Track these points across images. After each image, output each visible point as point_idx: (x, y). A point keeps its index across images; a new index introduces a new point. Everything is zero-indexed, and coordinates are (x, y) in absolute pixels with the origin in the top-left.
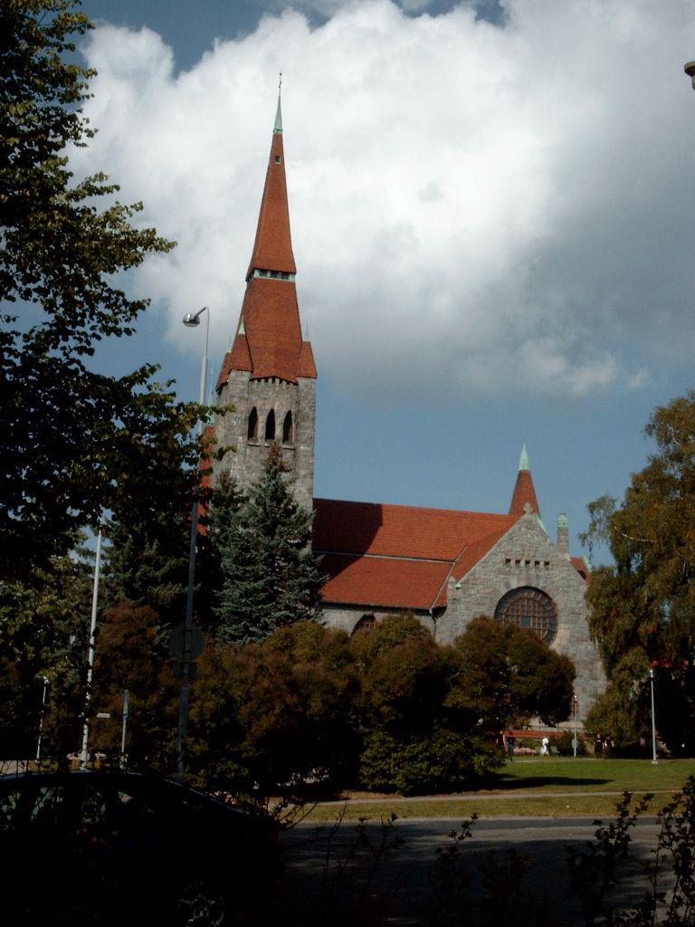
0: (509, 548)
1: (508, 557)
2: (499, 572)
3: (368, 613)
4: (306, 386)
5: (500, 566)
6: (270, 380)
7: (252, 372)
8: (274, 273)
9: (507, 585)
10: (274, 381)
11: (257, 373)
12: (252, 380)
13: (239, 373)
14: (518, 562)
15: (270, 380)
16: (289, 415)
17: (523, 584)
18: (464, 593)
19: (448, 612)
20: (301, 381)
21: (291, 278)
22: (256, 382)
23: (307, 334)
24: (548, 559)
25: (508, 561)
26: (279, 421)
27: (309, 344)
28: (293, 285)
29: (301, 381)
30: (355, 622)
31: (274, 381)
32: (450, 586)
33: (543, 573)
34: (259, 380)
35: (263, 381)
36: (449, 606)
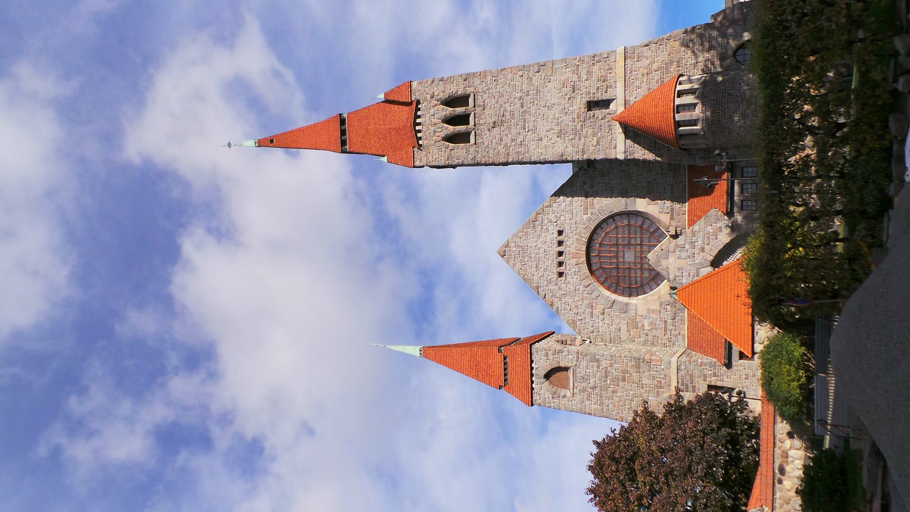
6: (418, 128)
15: (418, 128)
22: (421, 142)
26: (449, 111)
35: (419, 135)
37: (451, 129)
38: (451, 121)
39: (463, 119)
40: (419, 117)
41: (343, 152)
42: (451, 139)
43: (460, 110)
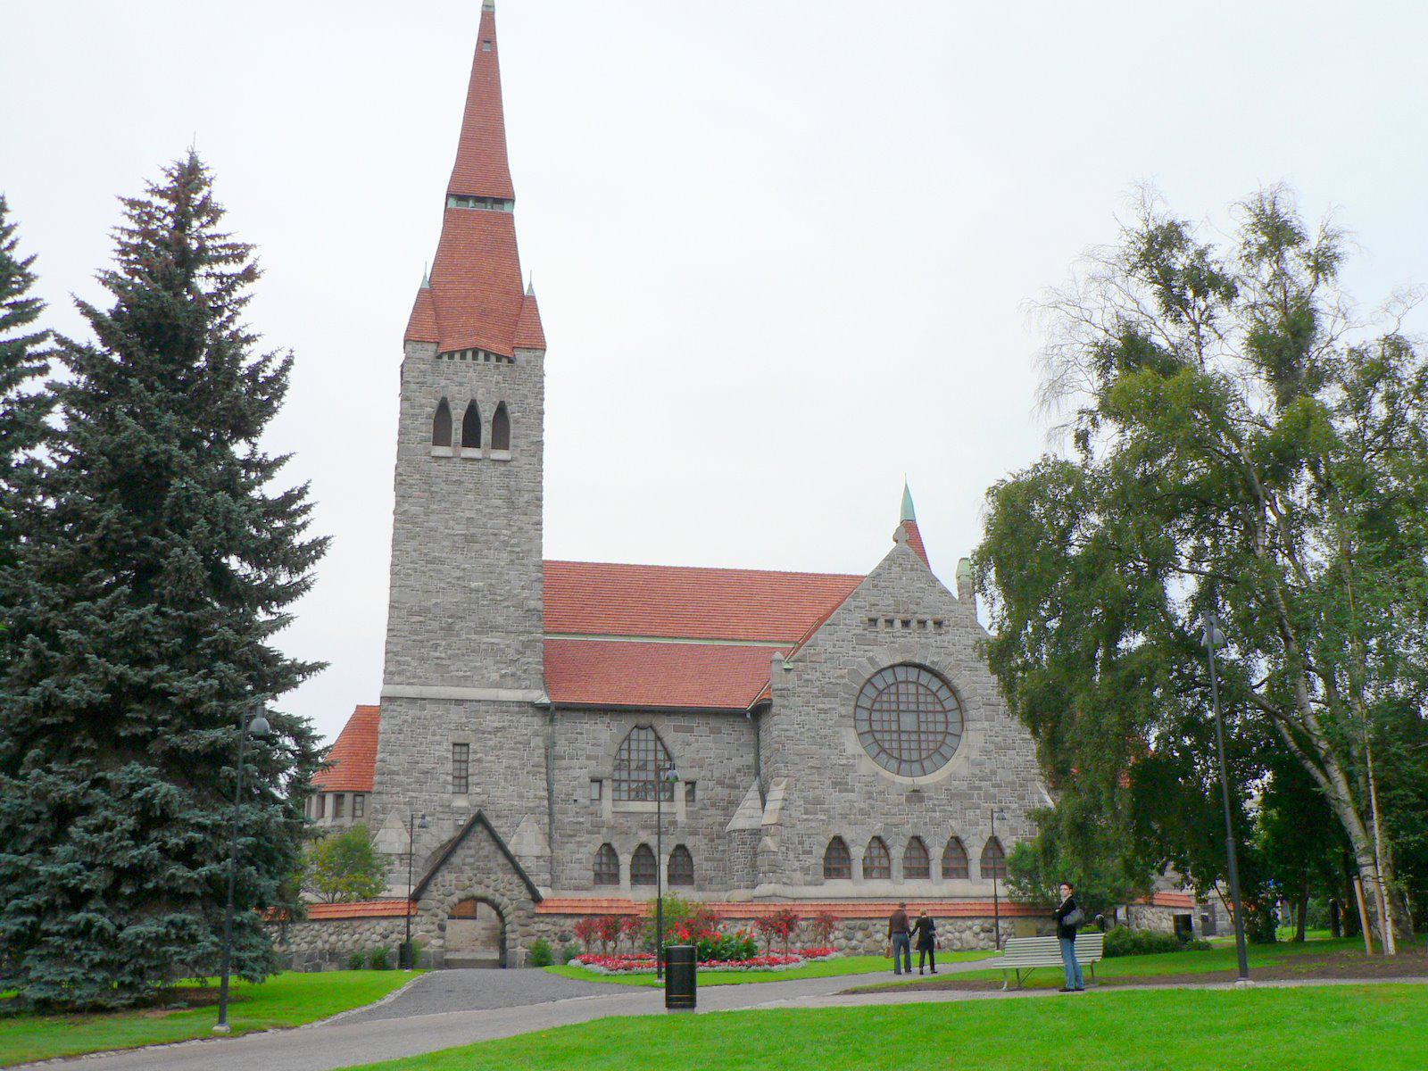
0: (872, 599)
1: (873, 615)
2: (861, 640)
3: (644, 720)
4: (528, 362)
6: (469, 354)
8: (480, 200)
9: (871, 660)
10: (475, 356)
11: (450, 344)
12: (440, 357)
13: (419, 346)
14: (890, 622)
15: (469, 354)
16: (501, 410)
17: (899, 660)
18: (799, 677)
19: (774, 710)
20: (521, 356)
21: (507, 208)
22: (445, 358)
23: (530, 285)
24: (939, 617)
26: (487, 414)
27: (533, 300)
28: (510, 217)
29: (521, 356)
31: (475, 356)
34: (451, 355)
35: (457, 356)
36: (776, 701)
37: (458, 414)
39: (471, 439)
40: (487, 358)
41: (449, 195)
42: (443, 408)
43: (486, 433)
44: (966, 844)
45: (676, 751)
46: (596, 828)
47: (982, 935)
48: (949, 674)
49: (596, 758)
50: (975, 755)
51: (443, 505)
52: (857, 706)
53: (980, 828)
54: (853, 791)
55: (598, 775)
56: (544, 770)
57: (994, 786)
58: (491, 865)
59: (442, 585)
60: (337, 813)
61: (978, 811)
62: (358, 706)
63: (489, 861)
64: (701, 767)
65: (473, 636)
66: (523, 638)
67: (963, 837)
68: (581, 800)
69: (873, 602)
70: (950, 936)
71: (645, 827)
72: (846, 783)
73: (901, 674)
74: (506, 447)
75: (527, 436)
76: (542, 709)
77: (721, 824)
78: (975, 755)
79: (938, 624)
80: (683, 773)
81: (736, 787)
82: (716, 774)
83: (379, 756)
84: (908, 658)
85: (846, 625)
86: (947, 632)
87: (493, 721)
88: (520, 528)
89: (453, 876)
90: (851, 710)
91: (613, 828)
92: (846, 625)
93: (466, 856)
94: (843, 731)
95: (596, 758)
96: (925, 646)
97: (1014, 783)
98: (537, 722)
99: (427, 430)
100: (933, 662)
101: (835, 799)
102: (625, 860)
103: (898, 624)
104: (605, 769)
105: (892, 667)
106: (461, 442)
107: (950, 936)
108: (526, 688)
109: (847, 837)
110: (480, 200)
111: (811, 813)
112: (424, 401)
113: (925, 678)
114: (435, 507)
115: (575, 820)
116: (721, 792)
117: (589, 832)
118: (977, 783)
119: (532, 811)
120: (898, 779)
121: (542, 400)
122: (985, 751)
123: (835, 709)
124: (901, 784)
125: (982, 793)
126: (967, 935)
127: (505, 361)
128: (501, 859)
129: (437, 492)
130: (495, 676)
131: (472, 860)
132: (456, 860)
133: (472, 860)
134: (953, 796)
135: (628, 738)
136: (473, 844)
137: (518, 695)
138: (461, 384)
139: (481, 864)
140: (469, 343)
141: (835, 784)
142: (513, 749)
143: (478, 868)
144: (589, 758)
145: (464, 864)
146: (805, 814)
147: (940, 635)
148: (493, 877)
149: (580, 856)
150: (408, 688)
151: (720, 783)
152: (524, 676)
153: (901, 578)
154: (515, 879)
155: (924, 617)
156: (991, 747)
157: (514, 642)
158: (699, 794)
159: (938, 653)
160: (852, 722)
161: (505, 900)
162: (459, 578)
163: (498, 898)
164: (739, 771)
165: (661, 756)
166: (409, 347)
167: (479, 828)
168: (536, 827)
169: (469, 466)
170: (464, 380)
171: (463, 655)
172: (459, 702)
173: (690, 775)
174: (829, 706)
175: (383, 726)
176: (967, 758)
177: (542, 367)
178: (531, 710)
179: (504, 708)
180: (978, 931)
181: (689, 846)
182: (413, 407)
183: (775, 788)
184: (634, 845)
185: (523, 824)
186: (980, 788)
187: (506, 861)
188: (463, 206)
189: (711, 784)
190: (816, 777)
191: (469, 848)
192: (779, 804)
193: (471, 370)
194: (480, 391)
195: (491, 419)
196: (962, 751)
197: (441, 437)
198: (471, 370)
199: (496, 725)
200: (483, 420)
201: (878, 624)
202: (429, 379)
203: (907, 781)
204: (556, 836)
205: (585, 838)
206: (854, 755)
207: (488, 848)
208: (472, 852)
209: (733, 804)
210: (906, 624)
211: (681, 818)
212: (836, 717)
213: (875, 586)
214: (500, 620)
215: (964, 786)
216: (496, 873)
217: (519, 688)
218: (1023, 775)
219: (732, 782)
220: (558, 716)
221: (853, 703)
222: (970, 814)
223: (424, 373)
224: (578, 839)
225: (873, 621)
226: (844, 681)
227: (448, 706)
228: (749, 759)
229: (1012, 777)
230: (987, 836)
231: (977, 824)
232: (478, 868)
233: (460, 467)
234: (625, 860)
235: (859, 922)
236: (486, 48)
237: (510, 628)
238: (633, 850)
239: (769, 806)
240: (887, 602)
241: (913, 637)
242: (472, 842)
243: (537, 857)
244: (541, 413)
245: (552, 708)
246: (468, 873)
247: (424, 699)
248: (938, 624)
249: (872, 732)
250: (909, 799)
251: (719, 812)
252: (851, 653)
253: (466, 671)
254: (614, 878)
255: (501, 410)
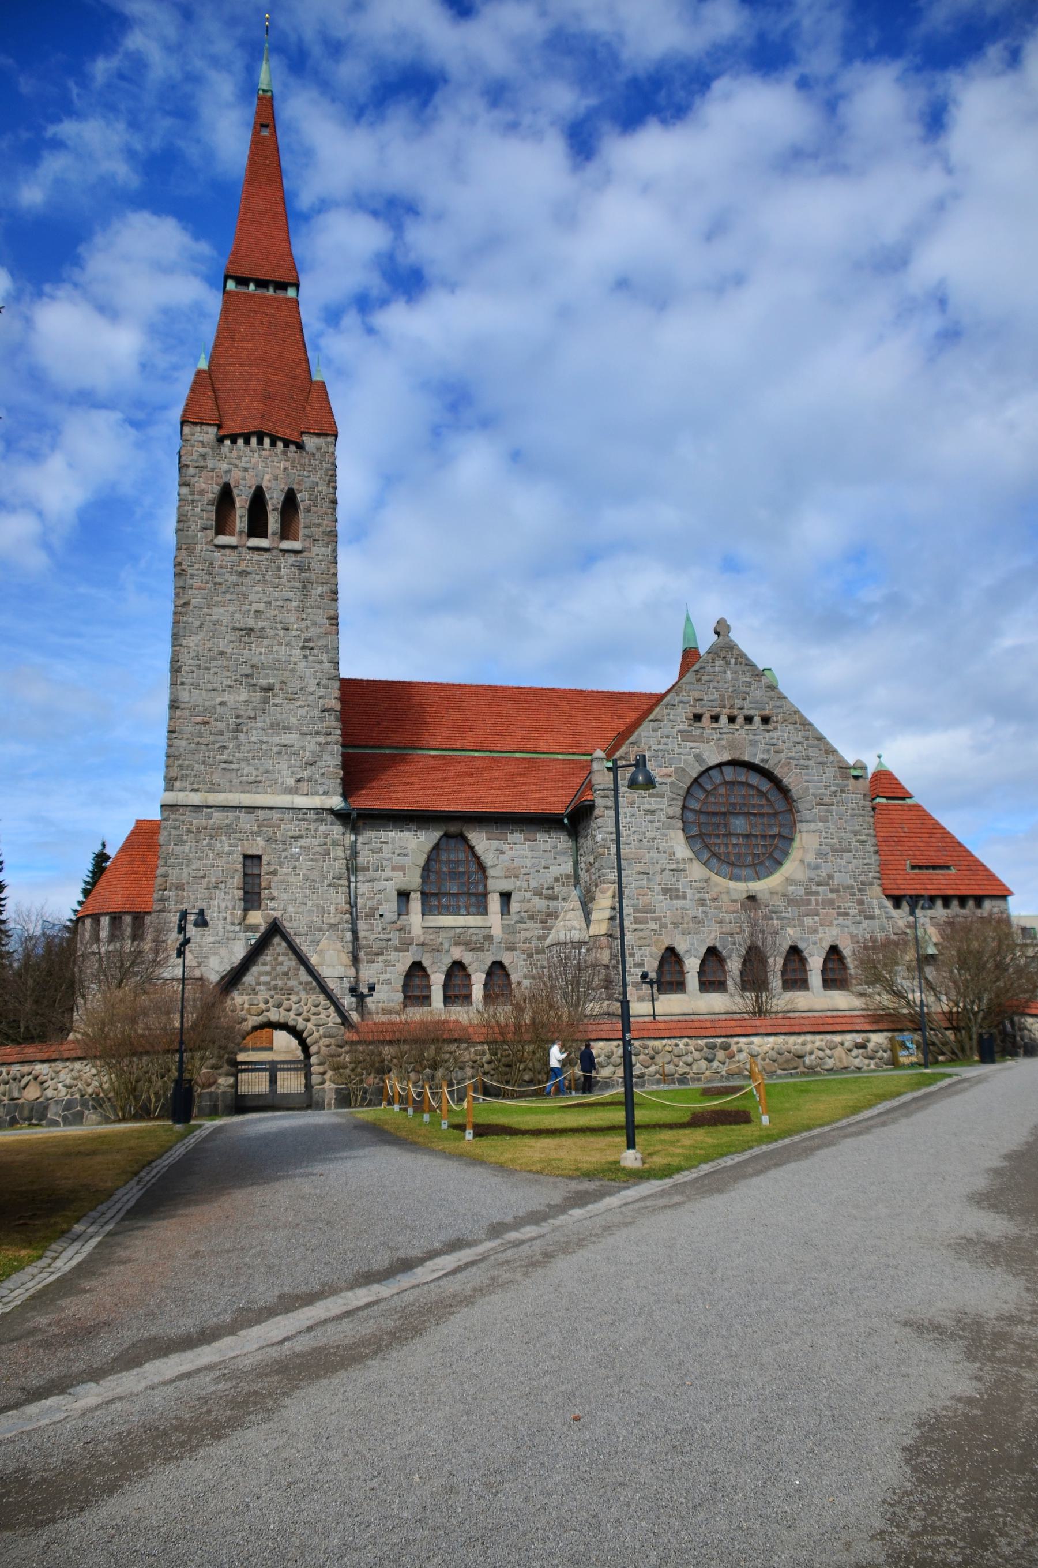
0: (697, 695)
2: (687, 737)
3: (453, 829)
4: (319, 449)
5: (684, 726)
6: (254, 441)
7: (219, 427)
8: (262, 284)
9: (698, 758)
10: (260, 442)
11: (232, 427)
12: (220, 440)
13: (198, 429)
14: (715, 718)
15: (254, 441)
16: (290, 501)
17: (726, 757)
21: (291, 293)
22: (227, 442)
24: (767, 712)
25: (698, 717)
26: (274, 500)
30: (429, 846)
31: (260, 442)
32: (596, 766)
33: (763, 737)
34: (234, 442)
37: (242, 502)
38: (258, 499)
39: (257, 526)
40: (273, 444)
41: (227, 277)
43: (273, 523)
44: (806, 954)
45: (488, 859)
46: (404, 946)
47: (855, 1052)
48: (777, 772)
49: (401, 868)
50: (811, 858)
51: (228, 596)
52: (684, 808)
53: (820, 935)
54: (684, 898)
55: (404, 887)
56: (346, 883)
57: (832, 891)
58: (292, 983)
59: (229, 683)
60: (112, 938)
61: (816, 917)
62: (138, 821)
63: (289, 979)
64: (517, 877)
65: (265, 739)
66: (321, 739)
67: (801, 945)
68: (387, 914)
69: (697, 697)
70: (821, 1054)
71: (457, 944)
72: (677, 890)
73: (729, 773)
74: (296, 538)
75: (319, 525)
76: (342, 816)
77: (539, 938)
78: (811, 858)
79: (766, 720)
80: (497, 884)
81: (556, 898)
82: (533, 884)
83: (160, 871)
84: (737, 756)
85: (670, 721)
86: (775, 729)
87: (289, 829)
88: (314, 623)
89: (246, 998)
90: (678, 810)
91: (423, 944)
92: (670, 721)
93: (260, 974)
94: (672, 833)
95: (401, 868)
96: (753, 743)
97: (852, 887)
98: (337, 829)
99: (210, 516)
100: (763, 760)
101: (664, 906)
102: (437, 979)
103: (724, 720)
104: (413, 880)
105: (720, 765)
106: (246, 530)
107: (821, 1054)
108: (324, 793)
109: (681, 948)
110: (262, 284)
111: (640, 923)
112: (204, 486)
113: (755, 779)
114: (219, 599)
115: (382, 936)
116: (540, 904)
117: (398, 950)
118: (814, 888)
119: (332, 927)
120: (732, 885)
121: (335, 488)
122: (820, 854)
123: (662, 810)
124: (736, 890)
125: (820, 898)
126: (839, 1051)
127: (293, 448)
128: (304, 976)
129: (220, 584)
130: (291, 782)
131: (267, 979)
132: (248, 979)
133: (267, 979)
134: (791, 901)
135: (436, 847)
136: (269, 958)
137: (317, 801)
138: (246, 470)
139: (280, 983)
140: (255, 425)
141: (665, 891)
142: (312, 860)
143: (275, 988)
144: (394, 869)
145: (259, 984)
146: (635, 923)
147: (768, 731)
148: (294, 998)
149: (387, 976)
150: (192, 794)
151: (538, 894)
152: (320, 780)
153: (725, 672)
154: (322, 998)
155: (752, 712)
156: (828, 849)
157: (311, 744)
158: (514, 906)
159: (768, 751)
160: (680, 824)
161: (310, 1025)
162: (247, 676)
163: (300, 1024)
164: (557, 880)
165: (473, 868)
166: (187, 430)
167: (277, 940)
168: (339, 945)
169: (257, 556)
170: (248, 465)
171: (254, 758)
172: (251, 809)
173: (505, 885)
174: (657, 807)
175: (162, 838)
176: (802, 861)
177: (333, 453)
178: (330, 818)
179: (300, 816)
180: (850, 1047)
181: (506, 962)
182: (192, 493)
183: (601, 895)
184: (446, 962)
185: (324, 942)
186: (817, 893)
187: (310, 979)
188: (242, 289)
189: (528, 895)
190: (645, 883)
191: (265, 964)
192: (607, 914)
193: (256, 455)
194: (267, 477)
195: (279, 506)
196: (796, 853)
197: (222, 526)
198: (256, 455)
199: (291, 834)
200: (270, 508)
201: (704, 719)
202: (210, 464)
203: (740, 888)
204: (362, 955)
205: (393, 956)
206: (684, 860)
207: (289, 962)
208: (268, 968)
209: (552, 915)
210: (732, 719)
211: (497, 932)
212: (663, 818)
213: (699, 680)
214: (294, 721)
215: (801, 891)
216: (297, 993)
217: (316, 793)
218: (862, 878)
219: (550, 892)
220: (360, 824)
221: (680, 803)
222: (808, 921)
223: (204, 456)
224: (384, 957)
225: (698, 717)
226: (669, 780)
227: (237, 814)
228: (568, 868)
229: (850, 882)
230: (826, 945)
231: (816, 931)
232: (275, 988)
233: (247, 555)
234: (437, 979)
235: (719, 1040)
236: (265, 133)
237: (305, 730)
238: (445, 969)
239: (594, 916)
240: (712, 697)
241: (741, 733)
242: (268, 957)
243: (341, 978)
244: (335, 502)
245: (354, 815)
246: (263, 994)
247: (211, 807)
248: (766, 720)
249: (701, 835)
250: (743, 904)
251: (538, 925)
252: (677, 750)
253: (257, 776)
254: (425, 999)
255: (290, 501)
